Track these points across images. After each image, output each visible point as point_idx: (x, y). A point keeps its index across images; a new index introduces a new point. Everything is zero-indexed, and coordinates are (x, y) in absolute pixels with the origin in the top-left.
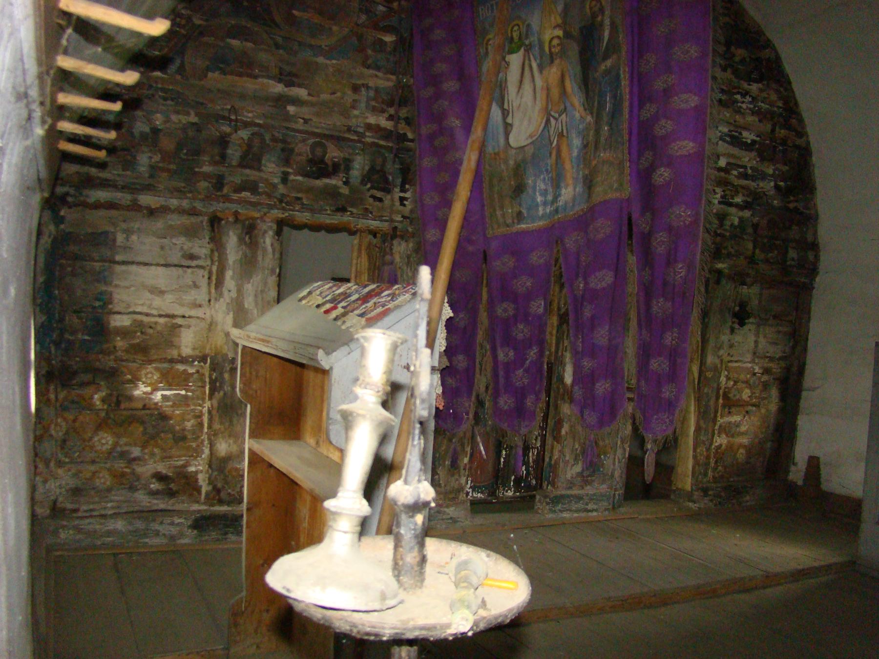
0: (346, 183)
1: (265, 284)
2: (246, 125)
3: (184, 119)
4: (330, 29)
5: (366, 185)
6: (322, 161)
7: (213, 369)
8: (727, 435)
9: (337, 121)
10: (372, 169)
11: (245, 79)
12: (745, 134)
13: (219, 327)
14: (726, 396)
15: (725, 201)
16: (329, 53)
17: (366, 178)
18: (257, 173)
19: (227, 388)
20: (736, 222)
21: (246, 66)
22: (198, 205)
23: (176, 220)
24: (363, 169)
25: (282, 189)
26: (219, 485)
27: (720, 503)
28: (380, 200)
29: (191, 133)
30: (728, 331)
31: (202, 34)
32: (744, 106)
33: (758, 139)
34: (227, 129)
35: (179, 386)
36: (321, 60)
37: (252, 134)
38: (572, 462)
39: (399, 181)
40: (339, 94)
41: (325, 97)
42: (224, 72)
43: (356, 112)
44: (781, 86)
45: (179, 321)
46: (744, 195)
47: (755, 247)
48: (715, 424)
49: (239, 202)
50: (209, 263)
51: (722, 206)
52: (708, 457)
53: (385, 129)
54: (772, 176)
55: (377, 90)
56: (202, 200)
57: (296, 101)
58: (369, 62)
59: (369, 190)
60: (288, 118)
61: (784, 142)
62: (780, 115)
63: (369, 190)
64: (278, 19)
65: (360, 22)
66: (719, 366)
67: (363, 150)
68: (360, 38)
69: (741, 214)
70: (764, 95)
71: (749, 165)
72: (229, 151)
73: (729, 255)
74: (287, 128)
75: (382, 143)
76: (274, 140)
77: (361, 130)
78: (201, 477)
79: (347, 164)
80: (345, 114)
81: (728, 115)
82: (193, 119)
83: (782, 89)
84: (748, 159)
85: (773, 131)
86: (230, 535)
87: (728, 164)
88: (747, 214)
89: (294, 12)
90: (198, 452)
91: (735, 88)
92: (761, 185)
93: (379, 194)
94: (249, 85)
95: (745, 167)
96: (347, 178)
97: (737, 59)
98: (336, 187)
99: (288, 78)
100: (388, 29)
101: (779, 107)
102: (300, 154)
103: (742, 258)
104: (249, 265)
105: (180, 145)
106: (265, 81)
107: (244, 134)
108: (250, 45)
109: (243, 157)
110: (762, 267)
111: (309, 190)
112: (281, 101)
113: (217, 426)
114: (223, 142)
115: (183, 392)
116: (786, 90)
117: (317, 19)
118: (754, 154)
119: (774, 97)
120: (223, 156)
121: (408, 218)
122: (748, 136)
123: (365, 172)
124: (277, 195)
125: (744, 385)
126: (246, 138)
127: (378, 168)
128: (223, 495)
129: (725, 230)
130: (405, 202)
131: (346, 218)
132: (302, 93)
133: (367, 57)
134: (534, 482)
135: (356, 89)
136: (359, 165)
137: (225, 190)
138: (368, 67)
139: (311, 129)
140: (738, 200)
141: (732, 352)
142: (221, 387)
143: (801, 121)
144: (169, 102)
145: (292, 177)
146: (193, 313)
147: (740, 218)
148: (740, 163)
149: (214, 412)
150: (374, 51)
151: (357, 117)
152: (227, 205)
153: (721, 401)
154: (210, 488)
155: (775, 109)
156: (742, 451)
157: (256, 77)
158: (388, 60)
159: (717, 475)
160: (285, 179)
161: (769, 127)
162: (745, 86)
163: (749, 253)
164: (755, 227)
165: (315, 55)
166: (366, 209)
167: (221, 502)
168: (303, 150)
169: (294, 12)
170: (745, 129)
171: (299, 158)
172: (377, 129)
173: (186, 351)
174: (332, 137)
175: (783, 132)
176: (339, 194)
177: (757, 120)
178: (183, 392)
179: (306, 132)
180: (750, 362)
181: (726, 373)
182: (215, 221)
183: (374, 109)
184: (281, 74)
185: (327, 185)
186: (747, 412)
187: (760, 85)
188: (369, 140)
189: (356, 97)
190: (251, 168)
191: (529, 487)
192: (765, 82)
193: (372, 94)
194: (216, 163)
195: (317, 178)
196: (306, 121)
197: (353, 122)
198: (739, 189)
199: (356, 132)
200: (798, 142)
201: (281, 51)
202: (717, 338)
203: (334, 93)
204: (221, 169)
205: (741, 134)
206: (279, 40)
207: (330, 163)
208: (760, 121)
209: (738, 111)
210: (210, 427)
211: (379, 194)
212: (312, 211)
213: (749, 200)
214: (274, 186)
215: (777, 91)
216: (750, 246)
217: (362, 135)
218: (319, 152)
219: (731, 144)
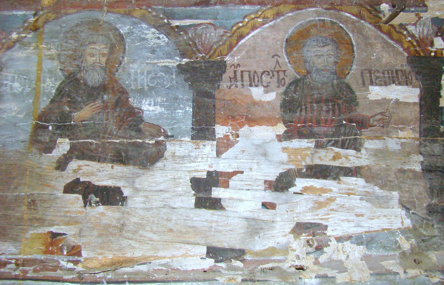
5: (49, 148)
10: (73, 88)
24: (37, 93)
28: (111, 196)
39: (185, 112)
59: (62, 165)
63: (62, 165)
67: (35, 29)
93: (103, 174)
121: (239, 254)
123: (45, 103)
127: (94, 78)
130: (217, 192)
211: (103, 174)
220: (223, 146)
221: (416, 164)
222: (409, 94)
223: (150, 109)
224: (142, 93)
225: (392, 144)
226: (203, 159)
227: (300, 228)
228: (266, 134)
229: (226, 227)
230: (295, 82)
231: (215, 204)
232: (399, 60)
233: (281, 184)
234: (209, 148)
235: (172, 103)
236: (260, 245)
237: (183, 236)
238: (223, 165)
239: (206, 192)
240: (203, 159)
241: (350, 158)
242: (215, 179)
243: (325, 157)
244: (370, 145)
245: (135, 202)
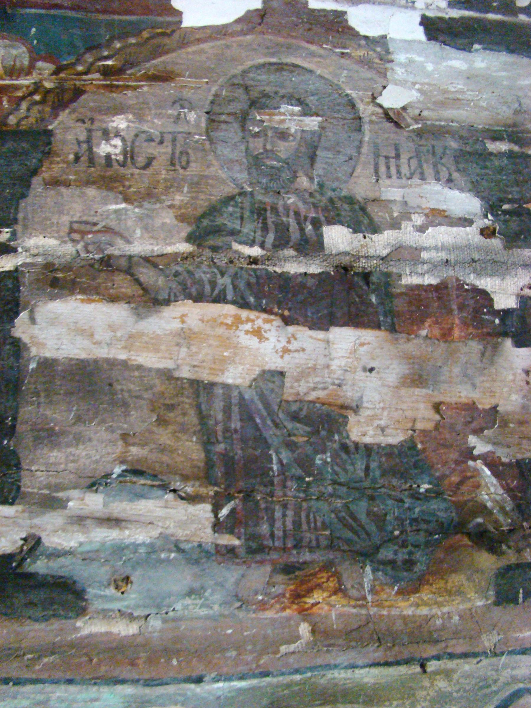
51: (483, 61)
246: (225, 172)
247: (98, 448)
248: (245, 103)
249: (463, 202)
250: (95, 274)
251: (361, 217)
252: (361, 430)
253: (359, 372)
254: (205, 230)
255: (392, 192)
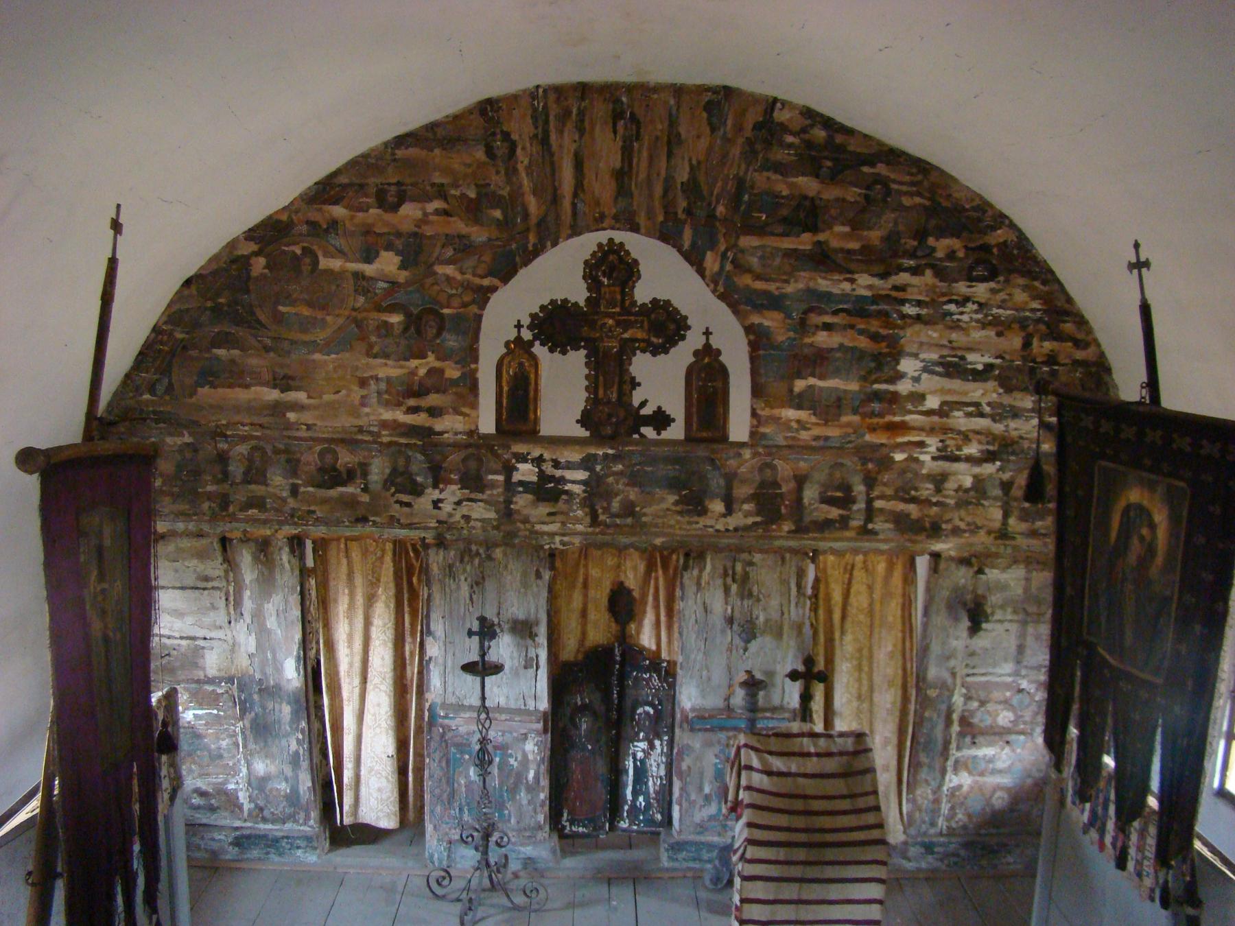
0: (365, 490)
1: (286, 602)
2: (244, 439)
3: (179, 441)
4: (323, 319)
5: (388, 490)
6: (334, 469)
7: (241, 690)
8: (970, 773)
9: (345, 422)
10: (394, 471)
11: (237, 389)
12: (971, 357)
13: (243, 649)
14: (964, 721)
15: (945, 455)
16: (327, 348)
17: (388, 482)
18: (263, 488)
19: (258, 709)
20: (968, 482)
21: (237, 376)
22: (206, 528)
23: (185, 543)
24: (383, 473)
25: (292, 503)
26: (261, 803)
27: (955, 864)
28: (409, 505)
29: (188, 455)
30: (965, 634)
31: (184, 348)
32: (965, 318)
33: (998, 361)
34: (223, 446)
35: (210, 706)
36: (317, 356)
37: (252, 448)
38: (701, 802)
39: (430, 481)
40: (344, 392)
41: (327, 397)
42: (213, 386)
43: (367, 410)
44: (1035, 279)
45: (201, 643)
46: (980, 442)
47: (1006, 515)
48: (947, 759)
49: (248, 520)
50: (224, 584)
52: (937, 801)
53: (404, 425)
54: (1032, 410)
55: (389, 380)
56: (210, 521)
57: (297, 407)
58: (376, 349)
59: (393, 495)
60: (289, 426)
61: (1051, 359)
62: (1039, 321)
63: (393, 495)
64: (262, 317)
65: (358, 305)
66: (950, 681)
68: (359, 324)
69: (976, 470)
70: (1002, 296)
71: (984, 402)
72: (231, 468)
73: (956, 531)
74: (289, 437)
75: (403, 441)
76: (277, 451)
77: (376, 429)
78: (241, 794)
79: (364, 468)
80: (355, 413)
81: (935, 335)
82: (188, 439)
83: (1037, 284)
84: (984, 393)
85: (1027, 344)
86: (272, 856)
87: (944, 403)
88: (989, 469)
89: (281, 308)
90: (235, 771)
91: (943, 295)
92: (1013, 424)
93: (405, 498)
94: (241, 395)
95: (977, 405)
96: (366, 485)
97: (940, 254)
98: (353, 494)
99: (284, 382)
100: (392, 309)
101: (1033, 310)
102: (308, 464)
103: (982, 532)
104: (267, 583)
105: (180, 468)
106: (258, 388)
107: (243, 449)
108: (235, 352)
109: (246, 473)
110: (1022, 542)
111: (325, 501)
112: (278, 409)
113: (252, 746)
114: (223, 458)
115: (215, 712)
116: (1044, 283)
117: (306, 312)
118: (991, 384)
119: (1020, 296)
120: (226, 474)
121: (446, 522)
122: (977, 360)
124: (287, 509)
125: (1000, 707)
126: (245, 453)
127: (401, 469)
128: (266, 813)
129: (946, 497)
131: (368, 529)
132: (301, 396)
133: (371, 346)
134: (659, 817)
135: (363, 383)
136: (378, 469)
137: (231, 509)
138: (375, 357)
139: (316, 435)
140: (972, 449)
141: (975, 661)
142: (252, 708)
143: (1081, 322)
144: (162, 425)
145: (302, 489)
146: (213, 634)
147: (975, 477)
148: (968, 400)
149: (248, 733)
150: (379, 336)
151: (367, 415)
152: (234, 524)
153: (956, 728)
154: (252, 805)
155: (1027, 314)
156: (999, 794)
157: (247, 387)
158: (398, 345)
159: (954, 825)
160: (294, 491)
161: (1017, 342)
162: (962, 288)
163: (997, 525)
164: (1006, 486)
165: (313, 352)
166: (392, 517)
167: (265, 820)
168: (310, 459)
169: (281, 308)
170: (970, 350)
171: (306, 469)
172: (394, 426)
173: (212, 672)
174: (343, 441)
175: (1048, 345)
176: (358, 503)
177: (993, 333)
178: (215, 712)
179: (312, 439)
180: (1009, 675)
181: (964, 691)
182: (224, 542)
183: (387, 404)
184: (275, 379)
185: (342, 495)
186: (1008, 742)
187: (992, 285)
188: (385, 440)
189: (364, 392)
190: (256, 483)
191: (651, 822)
192: (1001, 279)
193: (383, 386)
194: (218, 482)
195: (331, 487)
196: (309, 427)
197: (362, 422)
198: (971, 435)
199: (370, 433)
200: (1080, 355)
201: (272, 354)
202: (943, 643)
203: (338, 392)
204: (226, 487)
205: (962, 358)
206: (268, 342)
207: (342, 469)
208: (999, 334)
209: (956, 326)
210: (245, 746)
212: (327, 523)
213: (991, 448)
214: (284, 500)
215: (1025, 288)
216: (997, 514)
217: (378, 435)
218: (329, 459)
219: (948, 375)
220: (442, 491)
221: (501, 499)
222: (501, 478)
223: (419, 479)
224: (417, 474)
225: (495, 492)
226: (436, 495)
227: (463, 517)
228: (454, 487)
229: (442, 515)
230: (465, 473)
231: (439, 508)
232: (499, 466)
233: (458, 503)
234: (437, 491)
235: (426, 478)
236: (452, 520)
237: (431, 517)
238: (441, 497)
239: (436, 504)
240: (436, 495)
241: (480, 496)
242: (440, 501)
243: (473, 496)
244: (488, 492)
245: (416, 507)
246: (899, 483)
247: (882, 518)
248: (903, 472)
249: (931, 486)
250: (882, 497)
251: (916, 489)
252: (913, 517)
253: (913, 510)
254: (896, 491)
255: (922, 485)
